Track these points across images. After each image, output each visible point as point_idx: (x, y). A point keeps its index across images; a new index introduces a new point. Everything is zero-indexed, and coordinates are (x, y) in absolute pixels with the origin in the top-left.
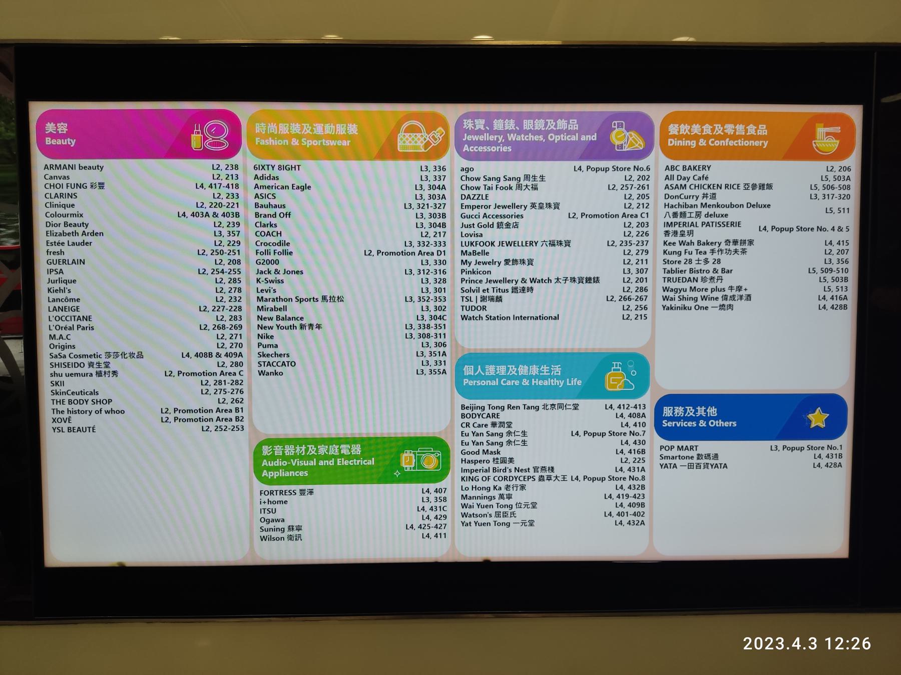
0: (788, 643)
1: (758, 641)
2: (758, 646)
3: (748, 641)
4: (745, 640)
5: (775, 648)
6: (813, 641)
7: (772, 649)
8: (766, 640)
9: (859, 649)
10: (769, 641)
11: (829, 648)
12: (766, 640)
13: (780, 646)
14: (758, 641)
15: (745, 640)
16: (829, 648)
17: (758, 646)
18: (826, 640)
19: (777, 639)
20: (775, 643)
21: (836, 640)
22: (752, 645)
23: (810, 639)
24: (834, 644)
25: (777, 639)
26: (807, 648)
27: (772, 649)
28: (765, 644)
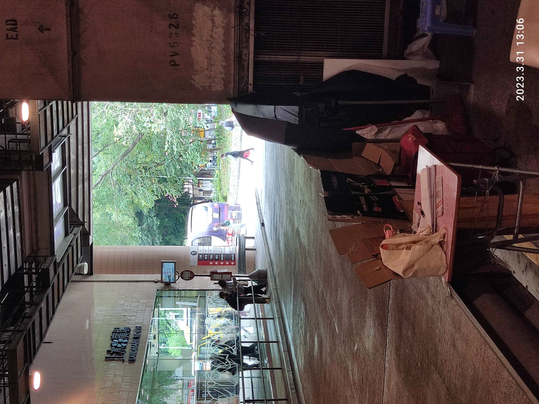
0: (520, 74)
1: (519, 92)
2: (522, 92)
3: (518, 98)
4: (518, 100)
5: (523, 82)
6: (518, 69)
7: (523, 83)
8: (518, 87)
9: (523, 96)
10: (518, 85)
11: (523, 43)
12: (518, 87)
13: (522, 79)
14: (519, 92)
15: (518, 100)
16: (523, 43)
17: (521, 92)
18: (518, 45)
19: (518, 81)
20: (520, 82)
21: (518, 39)
22: (521, 96)
23: (518, 71)
24: (520, 40)
25: (518, 81)
26: (523, 72)
27: (523, 83)
28: (520, 88)
